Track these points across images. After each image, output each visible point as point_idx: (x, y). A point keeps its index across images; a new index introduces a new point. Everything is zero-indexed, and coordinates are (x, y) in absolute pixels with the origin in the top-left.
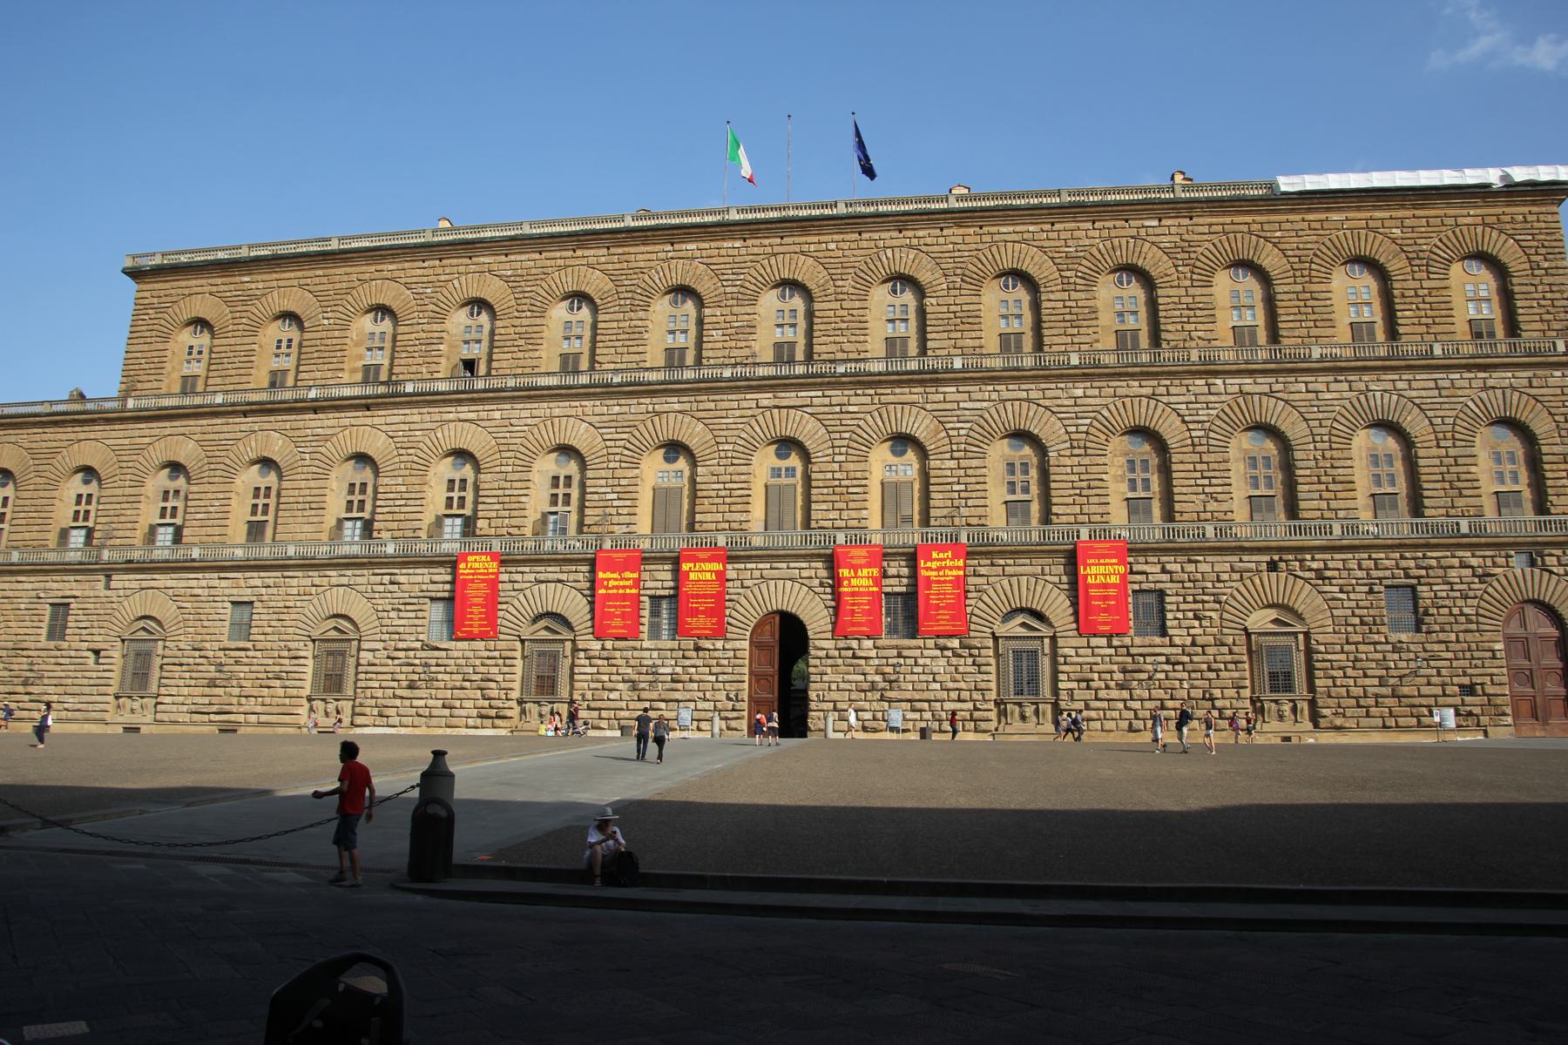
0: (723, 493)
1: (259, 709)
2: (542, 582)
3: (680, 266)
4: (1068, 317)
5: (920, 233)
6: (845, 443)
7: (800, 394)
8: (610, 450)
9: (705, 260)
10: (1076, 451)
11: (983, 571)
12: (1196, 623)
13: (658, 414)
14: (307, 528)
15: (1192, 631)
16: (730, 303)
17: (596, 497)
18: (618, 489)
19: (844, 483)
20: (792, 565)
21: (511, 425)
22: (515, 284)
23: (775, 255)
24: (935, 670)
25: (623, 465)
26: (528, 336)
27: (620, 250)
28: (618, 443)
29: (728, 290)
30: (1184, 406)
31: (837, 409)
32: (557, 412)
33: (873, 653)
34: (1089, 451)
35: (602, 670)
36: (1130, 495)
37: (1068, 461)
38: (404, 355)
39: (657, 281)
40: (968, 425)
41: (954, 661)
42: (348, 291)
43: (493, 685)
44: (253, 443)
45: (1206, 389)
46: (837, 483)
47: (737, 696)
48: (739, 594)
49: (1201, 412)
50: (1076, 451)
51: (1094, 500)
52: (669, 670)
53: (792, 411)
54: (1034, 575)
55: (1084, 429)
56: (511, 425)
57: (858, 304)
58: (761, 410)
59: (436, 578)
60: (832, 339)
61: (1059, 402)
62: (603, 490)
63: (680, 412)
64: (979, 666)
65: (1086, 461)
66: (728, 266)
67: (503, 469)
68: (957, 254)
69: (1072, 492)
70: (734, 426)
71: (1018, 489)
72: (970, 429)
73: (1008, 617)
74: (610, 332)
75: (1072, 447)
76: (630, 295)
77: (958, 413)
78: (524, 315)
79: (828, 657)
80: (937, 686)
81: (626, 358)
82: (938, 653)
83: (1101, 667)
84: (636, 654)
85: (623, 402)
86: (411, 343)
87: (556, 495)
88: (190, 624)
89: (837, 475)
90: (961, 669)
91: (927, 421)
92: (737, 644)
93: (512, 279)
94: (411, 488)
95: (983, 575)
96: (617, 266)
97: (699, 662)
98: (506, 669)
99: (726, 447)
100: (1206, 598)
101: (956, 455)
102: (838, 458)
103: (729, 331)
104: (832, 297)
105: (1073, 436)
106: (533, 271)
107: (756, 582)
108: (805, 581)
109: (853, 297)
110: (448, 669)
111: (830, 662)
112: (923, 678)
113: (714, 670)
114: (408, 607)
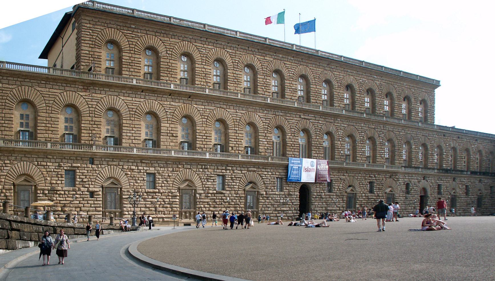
0: (293, 145)
1: (164, 216)
4: (360, 102)
5: (333, 67)
7: (310, 115)
11: (345, 174)
13: (276, 115)
14: (172, 144)
16: (291, 80)
17: (262, 142)
18: (268, 140)
19: (319, 145)
21: (237, 112)
27: (262, 52)
29: (291, 75)
31: (317, 122)
38: (198, 77)
40: (342, 131)
42: (176, 43)
44: (147, 104)
45: (383, 128)
46: (317, 145)
56: (237, 112)
58: (300, 119)
60: (314, 98)
61: (359, 127)
62: (264, 140)
66: (290, 66)
77: (341, 127)
78: (236, 69)
81: (266, 93)
84: (274, 196)
85: (267, 109)
86: (200, 72)
88: (132, 181)
89: (317, 143)
93: (231, 54)
98: (241, 201)
104: (314, 84)
113: (293, 201)
114: (212, 178)
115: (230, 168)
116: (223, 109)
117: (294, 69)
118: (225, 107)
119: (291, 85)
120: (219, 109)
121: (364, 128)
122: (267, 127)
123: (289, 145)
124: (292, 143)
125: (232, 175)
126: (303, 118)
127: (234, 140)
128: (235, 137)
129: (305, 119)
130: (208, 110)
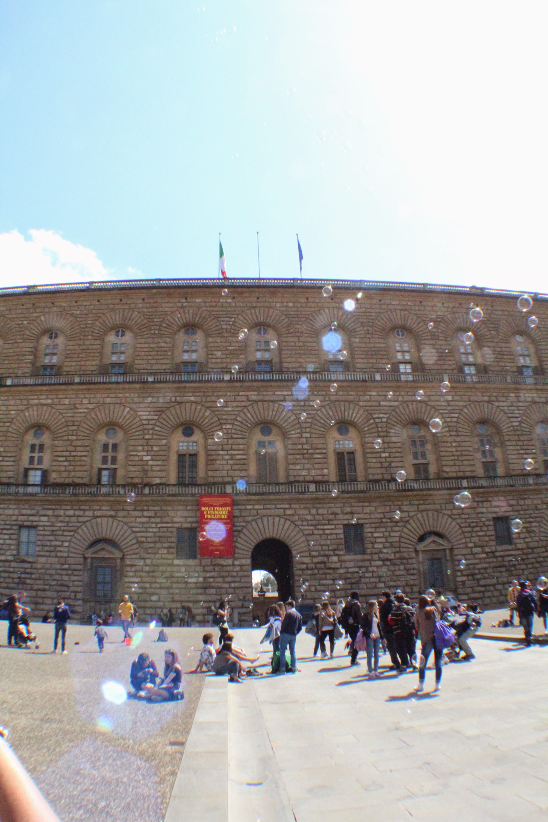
0: (227, 457)
2: (98, 517)
3: (191, 312)
6: (309, 425)
7: (276, 393)
8: (146, 427)
9: (209, 309)
10: (453, 433)
12: (527, 535)
13: (179, 403)
15: (527, 540)
18: (152, 453)
19: (310, 451)
20: (278, 506)
21: (76, 408)
22: (81, 319)
23: (254, 308)
24: (381, 574)
25: (155, 437)
26: (89, 351)
28: (151, 422)
29: (224, 327)
30: (506, 408)
32: (108, 400)
33: (338, 565)
34: (460, 434)
35: (144, 579)
36: (483, 460)
37: (449, 439)
39: (177, 319)
40: (387, 416)
41: (392, 568)
43: (66, 589)
47: (244, 597)
48: (242, 526)
49: (516, 412)
50: (453, 433)
51: (466, 463)
52: (194, 580)
53: (271, 404)
54: (436, 510)
55: (455, 420)
56: (76, 408)
57: (309, 339)
58: (251, 403)
59: (24, 512)
63: (195, 402)
64: (408, 570)
65: (458, 439)
67: (70, 437)
68: (368, 314)
69: (453, 458)
70: (232, 413)
71: (420, 457)
72: (388, 418)
73: (422, 539)
74: (145, 350)
75: (450, 431)
76: (158, 327)
79: (307, 569)
80: (382, 585)
82: (380, 563)
83: (480, 566)
84: (169, 569)
87: (107, 457)
89: (306, 446)
90: (397, 573)
91: (361, 412)
92: (243, 561)
94: (7, 449)
95: (406, 511)
96: (150, 310)
97: (216, 574)
99: (228, 426)
100: (532, 520)
101: (381, 434)
102: (305, 435)
103: (226, 352)
105: (450, 424)
106: (94, 311)
107: (254, 518)
108: (288, 517)
109: (306, 335)
110: (33, 576)
111: (309, 572)
112: (373, 580)
113: (229, 579)
115: (50, 513)
116: (45, 408)
117: (236, 316)
118: (49, 401)
119: (226, 344)
120: (35, 408)
121: (457, 403)
122: (151, 427)
123: (214, 457)
124: (225, 452)
125: (53, 526)
126: (257, 402)
127: (63, 459)
128: (67, 454)
129: (262, 401)
130: (13, 412)
